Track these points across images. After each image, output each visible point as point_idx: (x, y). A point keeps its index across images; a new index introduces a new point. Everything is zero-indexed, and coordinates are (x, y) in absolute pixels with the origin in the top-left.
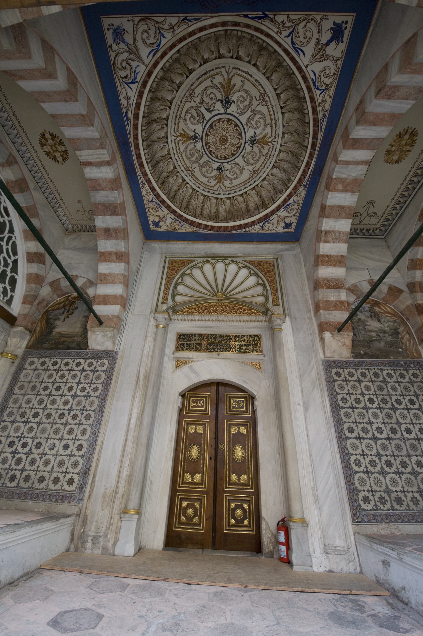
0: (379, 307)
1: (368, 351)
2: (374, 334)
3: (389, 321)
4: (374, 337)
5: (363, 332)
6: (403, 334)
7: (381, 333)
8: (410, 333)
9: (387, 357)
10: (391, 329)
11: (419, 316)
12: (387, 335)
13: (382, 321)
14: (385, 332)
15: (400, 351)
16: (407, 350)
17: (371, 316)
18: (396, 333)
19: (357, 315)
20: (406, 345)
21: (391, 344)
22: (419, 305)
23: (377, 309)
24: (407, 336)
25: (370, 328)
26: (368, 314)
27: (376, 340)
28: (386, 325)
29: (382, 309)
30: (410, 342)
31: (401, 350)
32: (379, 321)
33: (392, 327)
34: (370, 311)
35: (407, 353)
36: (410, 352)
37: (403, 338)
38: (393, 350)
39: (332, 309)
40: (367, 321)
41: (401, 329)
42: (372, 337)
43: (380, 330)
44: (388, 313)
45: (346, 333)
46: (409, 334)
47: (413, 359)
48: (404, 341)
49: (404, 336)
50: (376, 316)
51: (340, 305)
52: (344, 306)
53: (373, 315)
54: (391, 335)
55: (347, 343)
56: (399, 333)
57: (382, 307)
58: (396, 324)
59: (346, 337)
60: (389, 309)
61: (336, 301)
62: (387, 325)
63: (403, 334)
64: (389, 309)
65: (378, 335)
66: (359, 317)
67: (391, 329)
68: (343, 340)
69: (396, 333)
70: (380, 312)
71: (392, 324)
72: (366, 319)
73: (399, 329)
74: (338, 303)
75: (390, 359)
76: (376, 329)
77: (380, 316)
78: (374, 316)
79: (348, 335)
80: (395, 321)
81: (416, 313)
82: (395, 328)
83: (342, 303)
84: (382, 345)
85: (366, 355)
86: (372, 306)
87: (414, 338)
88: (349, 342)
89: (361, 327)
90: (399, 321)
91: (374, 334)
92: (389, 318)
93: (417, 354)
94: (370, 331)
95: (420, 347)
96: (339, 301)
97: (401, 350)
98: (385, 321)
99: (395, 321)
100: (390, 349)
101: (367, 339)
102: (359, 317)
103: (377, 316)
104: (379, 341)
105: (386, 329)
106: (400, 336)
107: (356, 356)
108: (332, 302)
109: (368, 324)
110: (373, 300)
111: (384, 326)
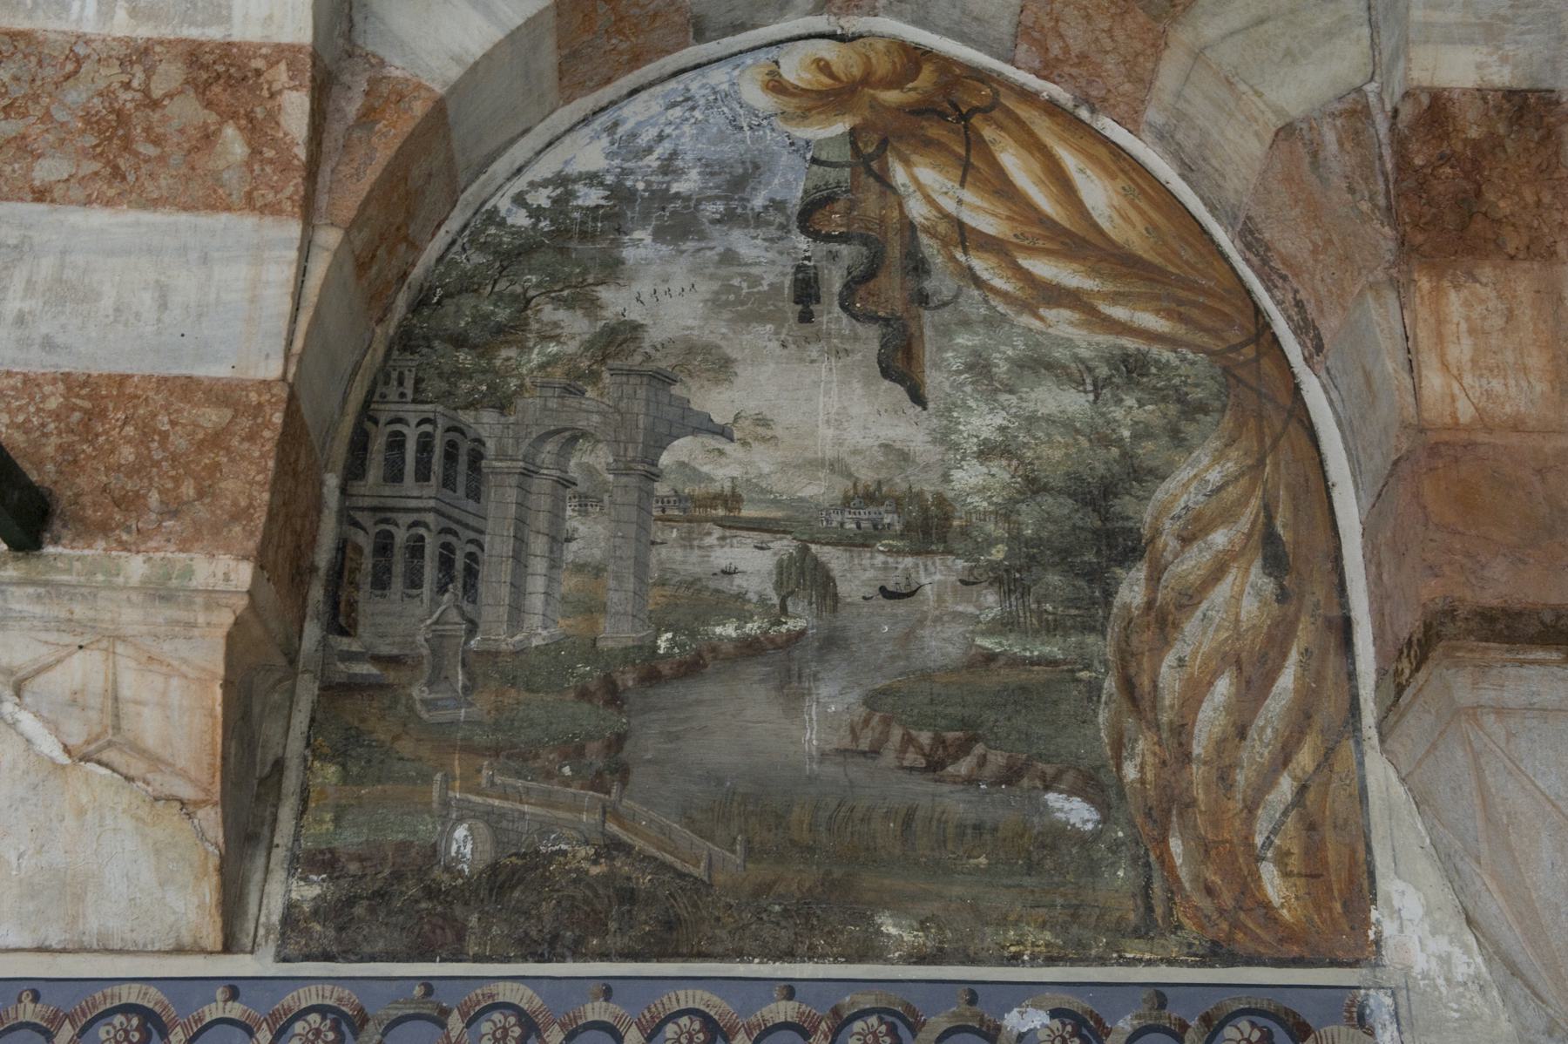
0: (974, 165)
1: (564, 821)
2: (752, 564)
3: (1038, 364)
4: (735, 605)
5: (590, 535)
6: (1191, 564)
7: (860, 541)
8: (1293, 553)
9: (823, 913)
10: (1033, 486)
11: (1401, 287)
12: (937, 575)
13: (942, 372)
14: (930, 527)
15: (1061, 835)
16: (1169, 804)
17: (806, 290)
18: (1088, 536)
19: (613, 269)
20: (1182, 731)
21: (950, 722)
22: (1436, 110)
23: (926, 186)
24: (1244, 597)
25: (723, 468)
26: (765, 258)
27: (750, 648)
28: (982, 423)
29: (1003, 189)
30: (1255, 686)
31: (1077, 812)
32: (900, 365)
33: (1052, 455)
34: (809, 216)
35: (1149, 861)
36: (1204, 849)
37: (1163, 621)
38: (956, 805)
39: (48, 170)
40: (722, 368)
41: (1198, 474)
42: (710, 598)
43: (871, 497)
44: (1080, 242)
45: (136, 567)
46: (1276, 559)
47: (1217, 954)
48: (1170, 679)
49: (1190, 598)
50: (875, 291)
51: (187, 111)
52: (258, 130)
53: (834, 280)
54: (1007, 580)
55: (149, 727)
56: (1126, 546)
57: (1013, 161)
58: (1129, 412)
59: (131, 617)
60: (1099, 194)
61: (140, 54)
62: (966, 442)
63: (1191, 564)
64: (1099, 194)
65: (806, 577)
66: (616, 302)
67: (1033, 486)
68: (82, 670)
69: (1088, 536)
70: (963, 236)
71: (1074, 402)
72: (717, 331)
73: (1141, 475)
74: (169, 75)
75: (867, 951)
76: (817, 489)
77: (941, 283)
78: (858, 282)
79: (160, 592)
80: (1132, 369)
81: (1384, 237)
82: (1101, 461)
83: (223, 74)
84: (812, 738)
85: (522, 900)
86: (868, 157)
87: (1345, 629)
88: (178, 709)
89: (595, 458)
90: (1190, 366)
91: (752, 564)
92: (1060, 321)
93: (1313, 874)
94: (725, 510)
95: (1379, 773)
96: (193, 54)
97: (1077, 812)
98: (979, 367)
99: (1131, 368)
100: (920, 789)
101: (617, 633)
102: (616, 302)
103: (891, 289)
104: (781, 660)
105: (968, 476)
106: (1132, 590)
107: (336, 912)
108: (75, 57)
109: (717, 403)
110: (915, 56)
111: (943, 438)
